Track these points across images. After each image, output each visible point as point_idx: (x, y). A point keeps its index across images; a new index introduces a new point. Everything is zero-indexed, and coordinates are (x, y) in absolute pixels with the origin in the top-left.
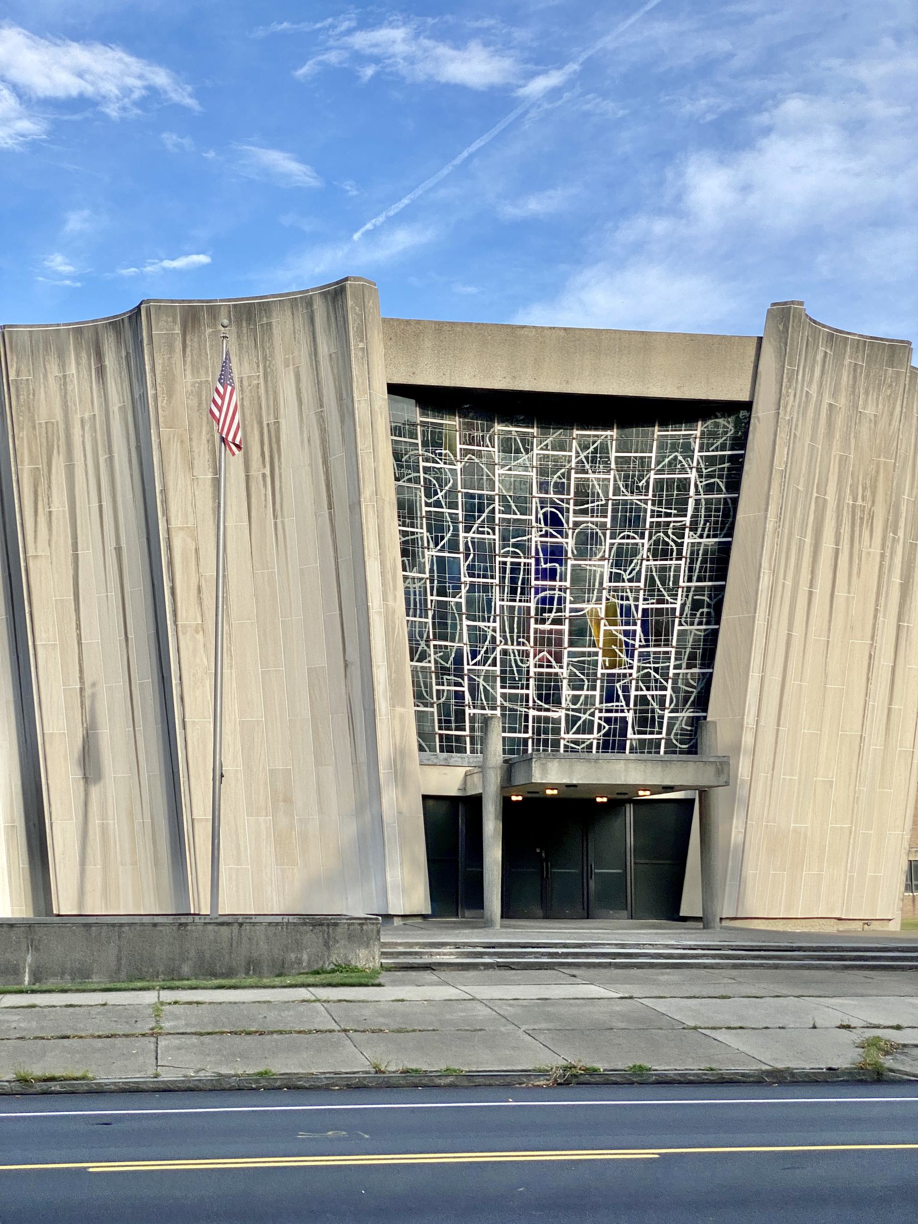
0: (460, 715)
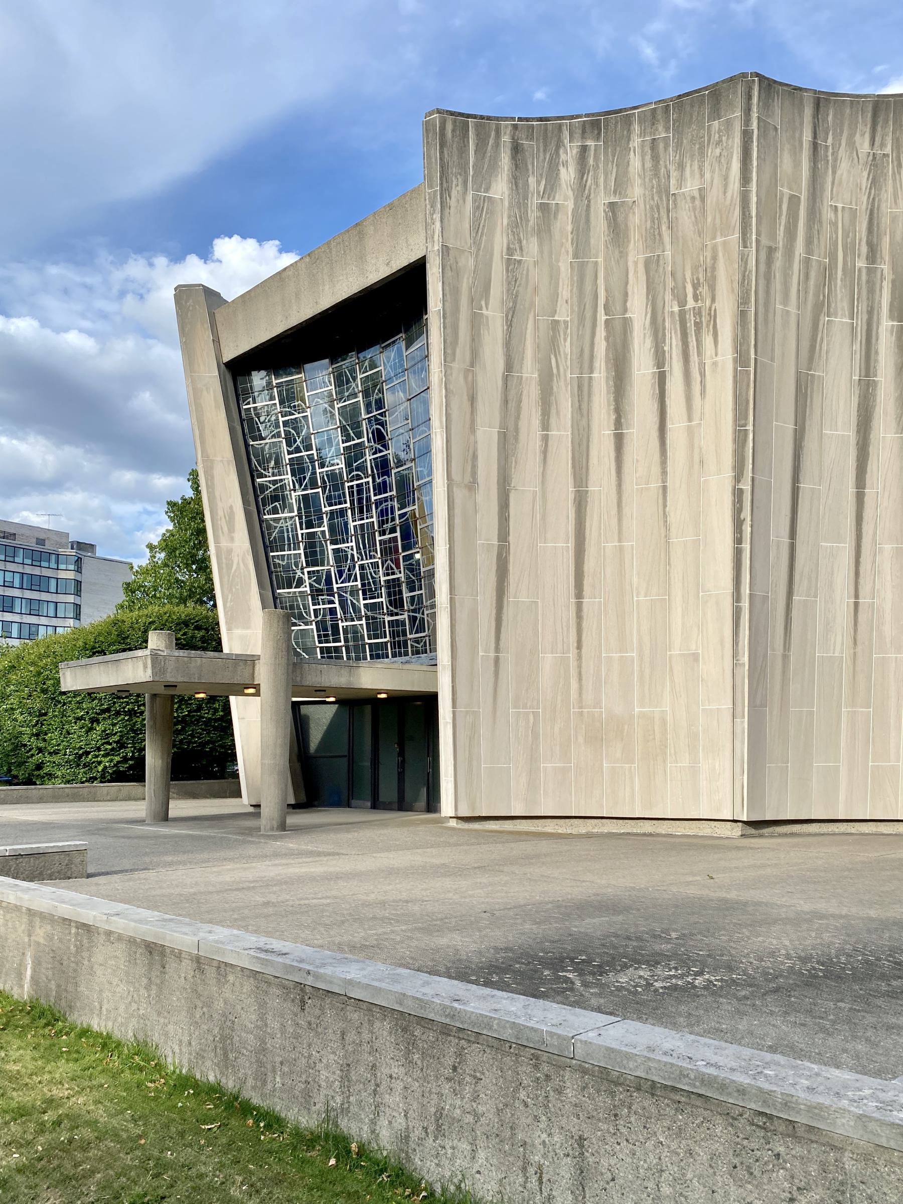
0: (335, 628)
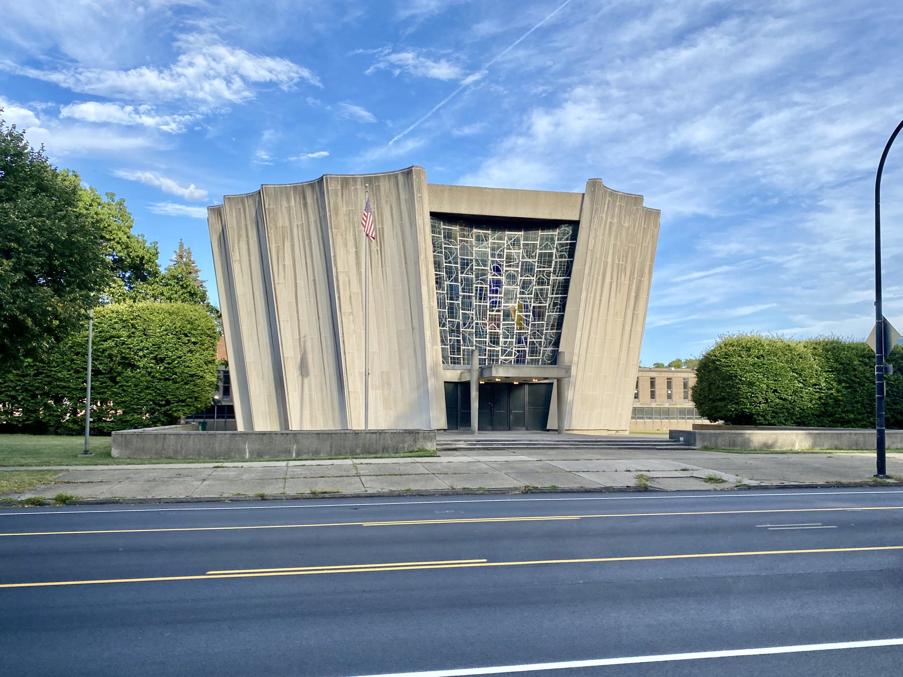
0: (459, 349)
